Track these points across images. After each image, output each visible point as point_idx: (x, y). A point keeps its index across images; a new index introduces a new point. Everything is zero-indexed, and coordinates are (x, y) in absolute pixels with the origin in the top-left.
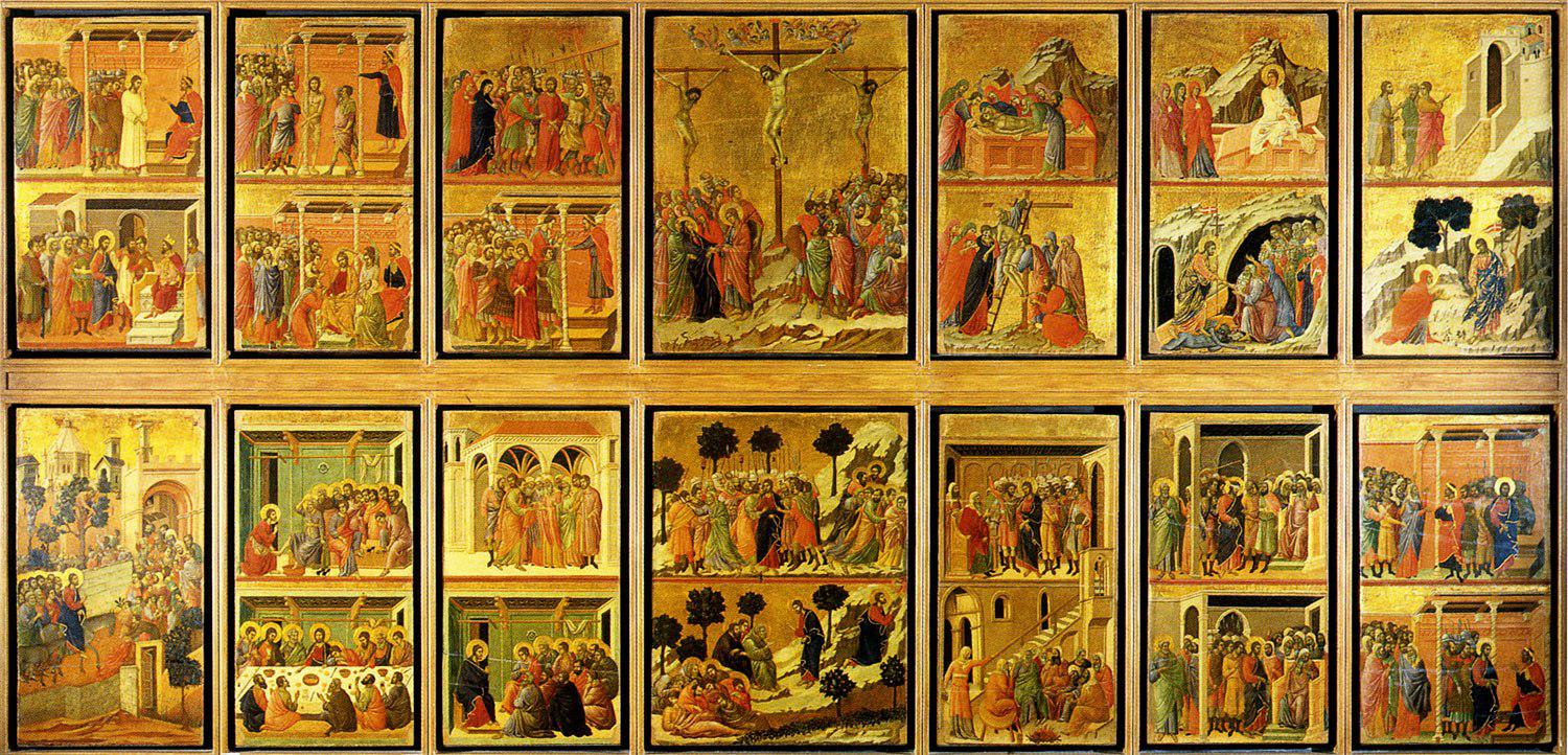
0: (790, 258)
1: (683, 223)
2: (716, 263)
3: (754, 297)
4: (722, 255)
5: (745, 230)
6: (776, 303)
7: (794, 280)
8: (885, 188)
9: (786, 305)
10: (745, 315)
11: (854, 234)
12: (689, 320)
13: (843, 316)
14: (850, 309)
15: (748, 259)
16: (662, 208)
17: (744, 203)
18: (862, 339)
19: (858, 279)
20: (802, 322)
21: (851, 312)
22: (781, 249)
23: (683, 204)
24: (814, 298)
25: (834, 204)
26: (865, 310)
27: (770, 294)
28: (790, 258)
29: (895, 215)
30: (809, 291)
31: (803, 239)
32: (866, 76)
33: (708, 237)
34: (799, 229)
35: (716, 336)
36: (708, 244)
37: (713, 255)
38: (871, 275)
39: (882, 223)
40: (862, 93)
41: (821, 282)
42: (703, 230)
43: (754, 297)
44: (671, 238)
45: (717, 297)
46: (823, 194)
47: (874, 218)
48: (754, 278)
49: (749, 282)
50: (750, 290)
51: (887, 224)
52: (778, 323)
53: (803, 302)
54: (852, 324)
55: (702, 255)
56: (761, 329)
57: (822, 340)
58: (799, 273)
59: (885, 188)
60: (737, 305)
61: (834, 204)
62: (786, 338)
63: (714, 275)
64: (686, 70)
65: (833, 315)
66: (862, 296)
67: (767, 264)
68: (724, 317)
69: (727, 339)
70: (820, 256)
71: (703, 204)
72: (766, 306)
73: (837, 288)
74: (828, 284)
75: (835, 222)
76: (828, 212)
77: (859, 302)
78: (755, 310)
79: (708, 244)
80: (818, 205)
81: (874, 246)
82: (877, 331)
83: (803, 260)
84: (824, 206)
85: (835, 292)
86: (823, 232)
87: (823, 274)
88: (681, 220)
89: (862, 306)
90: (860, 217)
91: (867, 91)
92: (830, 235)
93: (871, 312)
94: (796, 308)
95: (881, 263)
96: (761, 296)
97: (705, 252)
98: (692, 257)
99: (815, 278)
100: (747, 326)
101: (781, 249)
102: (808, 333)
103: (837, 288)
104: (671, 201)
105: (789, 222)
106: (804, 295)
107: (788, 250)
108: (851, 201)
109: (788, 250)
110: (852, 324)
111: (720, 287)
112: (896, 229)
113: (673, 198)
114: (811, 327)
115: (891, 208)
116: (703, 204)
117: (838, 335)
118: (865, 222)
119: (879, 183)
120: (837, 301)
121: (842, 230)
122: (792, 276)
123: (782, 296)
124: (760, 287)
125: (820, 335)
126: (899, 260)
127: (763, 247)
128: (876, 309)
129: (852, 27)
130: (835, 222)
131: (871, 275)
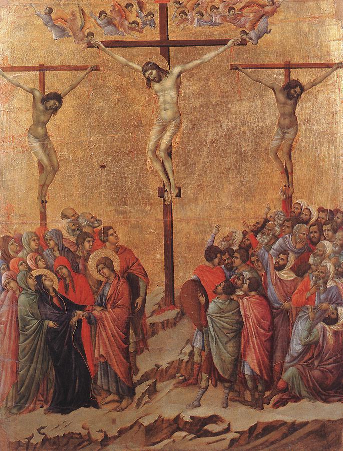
0: (186, 327)
1: (39, 278)
2: (85, 330)
3: (136, 378)
4: (92, 322)
5: (123, 287)
6: (166, 387)
7: (191, 354)
8: (314, 228)
9: (180, 389)
10: (124, 403)
11: (273, 292)
12: (48, 412)
13: (258, 404)
14: (267, 393)
15: (127, 327)
16: (10, 258)
17: (120, 250)
18: (285, 435)
19: (278, 354)
20: (202, 412)
21: (270, 398)
22: (171, 314)
23: (39, 252)
24: (218, 379)
25: (246, 250)
26: (290, 396)
27: (159, 374)
28: (186, 327)
29: (330, 266)
30: (212, 370)
31: (203, 300)
32: (288, 75)
33: (72, 297)
34: (196, 285)
35: (84, 432)
36: (73, 307)
37: (80, 321)
38: (296, 347)
39: (311, 279)
40: (282, 98)
41: (228, 357)
42: (66, 287)
43: (136, 378)
44: (22, 298)
45: (87, 379)
46: (229, 238)
47: (301, 269)
48: (138, 351)
49: (129, 357)
50: (132, 369)
51: (318, 278)
52: (169, 413)
53: (203, 384)
54: (269, 415)
55: (64, 322)
56: (146, 422)
57: (230, 436)
58: (198, 344)
59: (314, 228)
60: (113, 388)
61: (246, 250)
62: (180, 434)
63: (81, 346)
64: (42, 68)
65: (244, 402)
66: (286, 376)
67: (154, 333)
68: (96, 406)
69: (99, 437)
70: (226, 322)
71: (64, 250)
72: (152, 391)
73: (251, 365)
74: (238, 360)
75: (247, 275)
76: (237, 262)
77: (281, 384)
78: (137, 396)
79: (73, 307)
80: (222, 253)
81: (300, 307)
82: (306, 424)
83: (202, 327)
84: (231, 253)
85: (247, 371)
86: (230, 289)
87: (231, 347)
88: (35, 273)
89: (285, 390)
90: (280, 268)
91: (289, 96)
92: (240, 293)
93: (297, 399)
94: (192, 394)
95: (310, 331)
96: (145, 378)
97: (69, 318)
98: (51, 324)
99: (219, 353)
100: (129, 416)
101: (171, 314)
102: (210, 427)
103: (251, 365)
104: (21, 247)
105: (184, 275)
106: (205, 376)
107: (182, 314)
108: (268, 246)
109: (182, 314)
110: (269, 415)
111: (89, 363)
112: (330, 284)
113: (24, 242)
114: (214, 419)
115: (323, 256)
116: (64, 250)
117: (252, 429)
118: (287, 275)
119: (307, 222)
120: (250, 384)
121: (258, 286)
122: (188, 349)
123: (174, 377)
124: (145, 364)
125: (227, 430)
126: (334, 327)
127: (148, 309)
128: (304, 393)
129: (268, 8)
130: (247, 275)
131: (296, 347)
